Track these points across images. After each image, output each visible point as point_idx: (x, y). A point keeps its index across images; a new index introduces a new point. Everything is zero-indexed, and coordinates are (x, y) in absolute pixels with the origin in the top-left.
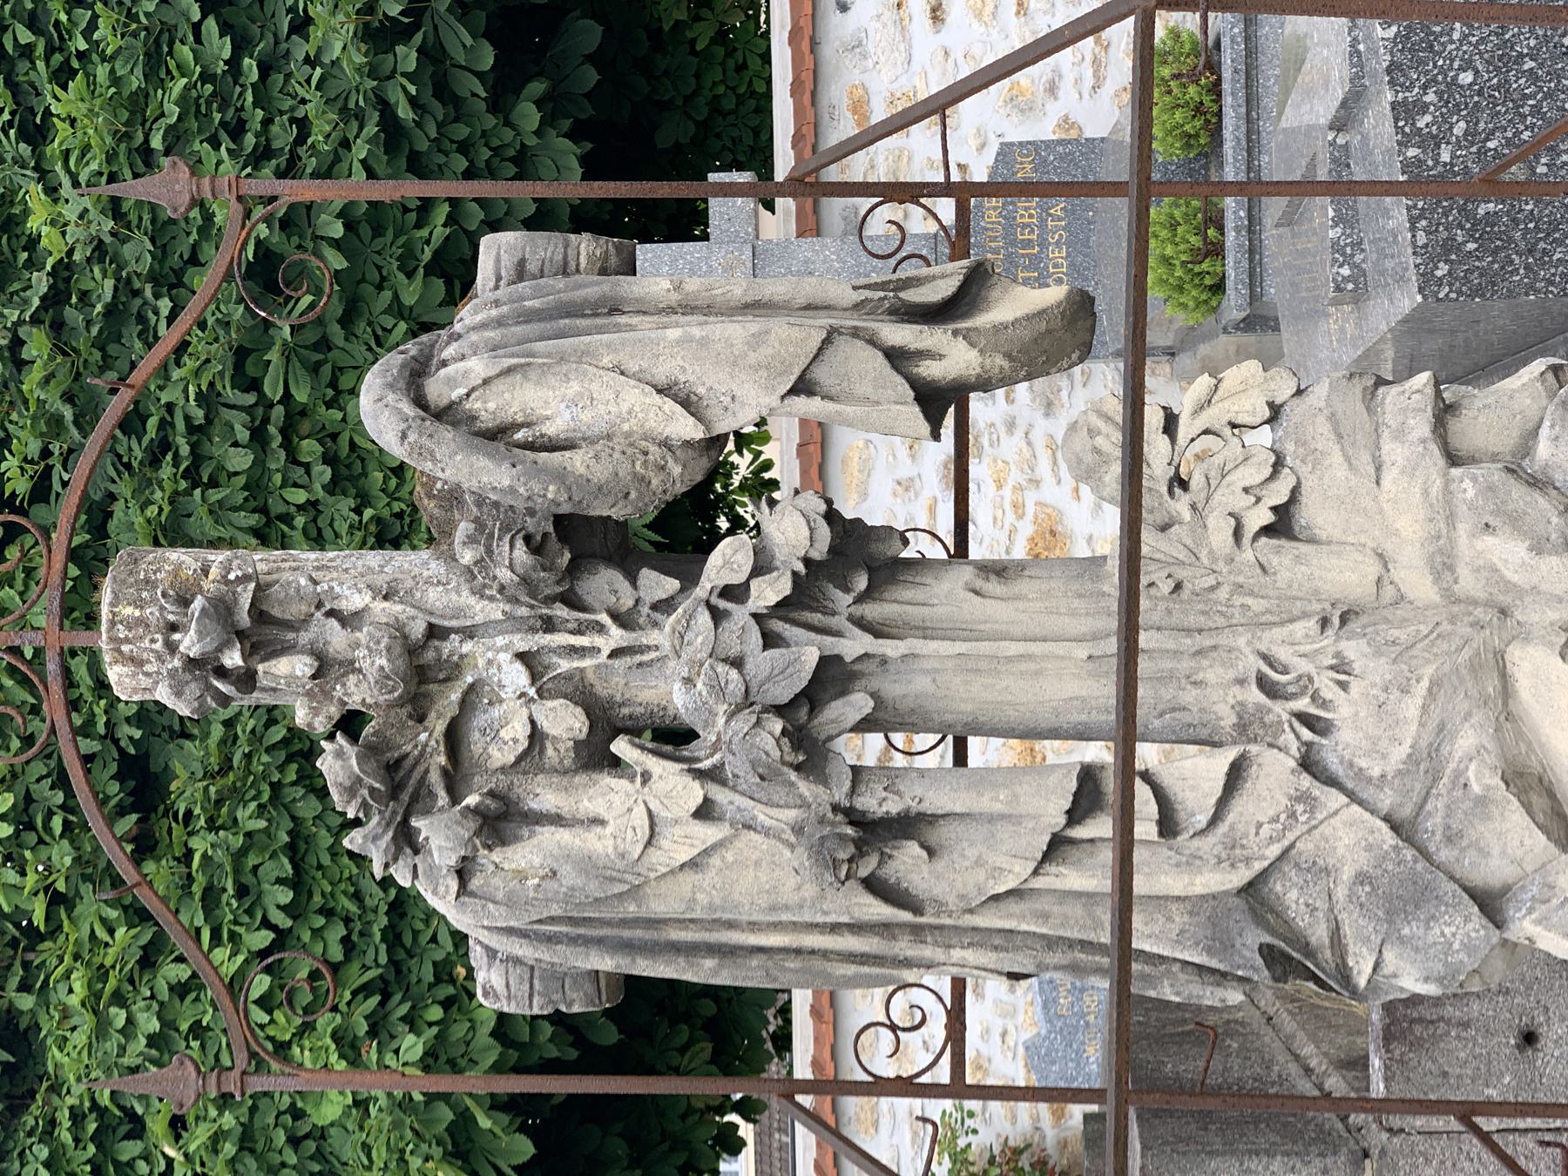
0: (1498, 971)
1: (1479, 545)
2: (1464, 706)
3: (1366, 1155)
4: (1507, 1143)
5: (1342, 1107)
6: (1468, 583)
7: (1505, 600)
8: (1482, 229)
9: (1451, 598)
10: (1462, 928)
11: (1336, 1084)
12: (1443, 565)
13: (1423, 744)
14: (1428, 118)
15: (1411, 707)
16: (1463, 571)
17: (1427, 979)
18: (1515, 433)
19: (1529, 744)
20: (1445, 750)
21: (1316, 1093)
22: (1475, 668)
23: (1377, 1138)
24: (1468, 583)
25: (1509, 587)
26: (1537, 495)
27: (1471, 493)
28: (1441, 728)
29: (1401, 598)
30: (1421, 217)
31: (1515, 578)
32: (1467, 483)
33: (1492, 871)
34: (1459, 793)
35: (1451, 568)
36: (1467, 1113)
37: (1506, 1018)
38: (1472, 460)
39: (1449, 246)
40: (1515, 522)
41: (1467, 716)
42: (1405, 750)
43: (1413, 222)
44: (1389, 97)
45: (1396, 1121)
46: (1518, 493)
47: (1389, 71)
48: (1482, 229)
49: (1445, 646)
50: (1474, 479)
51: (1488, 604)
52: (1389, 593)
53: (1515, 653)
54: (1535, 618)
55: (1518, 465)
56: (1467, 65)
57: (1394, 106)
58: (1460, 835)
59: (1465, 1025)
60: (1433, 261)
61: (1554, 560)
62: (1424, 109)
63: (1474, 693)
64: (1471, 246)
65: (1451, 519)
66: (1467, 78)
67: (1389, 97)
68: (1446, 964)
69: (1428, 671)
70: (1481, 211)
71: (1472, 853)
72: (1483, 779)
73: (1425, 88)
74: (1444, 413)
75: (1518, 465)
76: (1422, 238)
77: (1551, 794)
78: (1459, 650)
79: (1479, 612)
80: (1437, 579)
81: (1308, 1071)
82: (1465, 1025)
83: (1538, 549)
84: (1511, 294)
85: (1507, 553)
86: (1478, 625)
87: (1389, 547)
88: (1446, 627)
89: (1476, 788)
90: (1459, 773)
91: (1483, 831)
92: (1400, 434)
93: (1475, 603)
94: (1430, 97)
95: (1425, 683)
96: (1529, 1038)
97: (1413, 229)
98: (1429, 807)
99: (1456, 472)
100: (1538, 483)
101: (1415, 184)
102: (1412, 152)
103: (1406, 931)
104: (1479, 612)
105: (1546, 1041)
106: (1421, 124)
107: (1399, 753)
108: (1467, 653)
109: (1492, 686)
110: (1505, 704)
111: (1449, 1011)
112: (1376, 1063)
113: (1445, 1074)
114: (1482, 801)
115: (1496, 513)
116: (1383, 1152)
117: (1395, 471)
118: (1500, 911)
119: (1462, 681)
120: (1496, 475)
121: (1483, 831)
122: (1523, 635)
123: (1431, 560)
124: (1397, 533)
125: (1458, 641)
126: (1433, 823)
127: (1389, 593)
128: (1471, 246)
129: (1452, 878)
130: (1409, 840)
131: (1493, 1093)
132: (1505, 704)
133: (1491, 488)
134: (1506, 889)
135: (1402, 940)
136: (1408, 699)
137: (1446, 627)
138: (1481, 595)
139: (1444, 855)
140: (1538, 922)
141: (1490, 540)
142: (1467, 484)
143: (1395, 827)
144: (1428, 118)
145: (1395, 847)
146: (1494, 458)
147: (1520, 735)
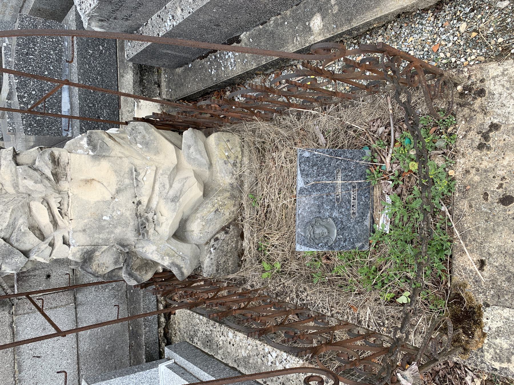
0: (30, 266)
1: (23, 182)
2: (20, 214)
3: (13, 305)
4: (35, 300)
5: (7, 295)
6: (21, 189)
7: (30, 193)
8: (37, 122)
9: (18, 192)
10: (20, 259)
11: (9, 291)
12: (16, 186)
13: (11, 222)
14: (25, 99)
15: (8, 215)
16: (20, 187)
17: (12, 270)
18: (32, 160)
19: (35, 221)
20: (16, 223)
21: (4, 294)
22: (23, 206)
23: (16, 301)
24: (21, 189)
25: (31, 190)
26: (35, 172)
27: (21, 171)
28: (15, 219)
29: (6, 193)
30: (24, 118)
31: (31, 188)
32: (20, 169)
33: (26, 247)
34: (19, 232)
35: (18, 186)
36: (27, 295)
37: (43, 273)
38: (22, 165)
39: (30, 125)
40: (31, 177)
41: (21, 216)
42: (7, 224)
43: (23, 119)
44: (17, 94)
45: (20, 297)
46: (31, 171)
47: (16, 89)
48: (37, 122)
49: (16, 202)
50: (21, 168)
51: (26, 194)
52: (4, 191)
53: (32, 203)
54: (36, 196)
55: (32, 167)
56: (34, 90)
57: (18, 96)
58: (19, 240)
59: (35, 276)
60: (27, 127)
61: (39, 185)
62: (25, 97)
63: (23, 211)
64: (35, 125)
65: (17, 176)
66: (34, 92)
67: (17, 94)
68: (16, 267)
69: (12, 207)
70: (37, 118)
71: (22, 244)
72: (24, 228)
73: (25, 93)
74: (15, 155)
75: (32, 167)
76: (24, 123)
77: (40, 230)
78: (19, 203)
79: (24, 195)
80: (15, 188)
81: (4, 289)
82: (35, 276)
83: (36, 182)
84: (44, 135)
85: (29, 183)
86: (24, 198)
87: (3, 182)
88: (16, 198)
89: (23, 230)
90: (19, 228)
91: (25, 239)
92: (5, 159)
93: (23, 193)
94: (26, 95)
95: (11, 210)
96: (48, 276)
97: (22, 120)
98: (13, 235)
99: (18, 167)
100: (35, 170)
101: (21, 111)
102: (22, 105)
103: (7, 261)
104: (24, 195)
105: (52, 277)
106: (24, 100)
107: (5, 225)
108: (21, 203)
109: (27, 210)
110: (30, 213)
111: (31, 273)
112: (16, 286)
113: (31, 286)
114: (24, 233)
115: (26, 175)
116: (17, 304)
117: (4, 166)
118: (29, 254)
119: (20, 209)
120: (26, 167)
121: (25, 239)
122: (34, 199)
123: (13, 184)
124: (5, 179)
125: (19, 201)
126: (13, 238)
127: (4, 191)
128: (35, 125)
129: (18, 249)
130: (8, 243)
131: (41, 288)
132: (30, 213)
133: (25, 170)
134: (30, 250)
135: (6, 263)
136: (7, 213)
137: (16, 198)
138: (25, 192)
139: (16, 244)
140: (37, 256)
141: (25, 181)
142: (20, 169)
143: (5, 240)
144: (25, 99)
145: (5, 244)
146: (27, 164)
147: (33, 219)
